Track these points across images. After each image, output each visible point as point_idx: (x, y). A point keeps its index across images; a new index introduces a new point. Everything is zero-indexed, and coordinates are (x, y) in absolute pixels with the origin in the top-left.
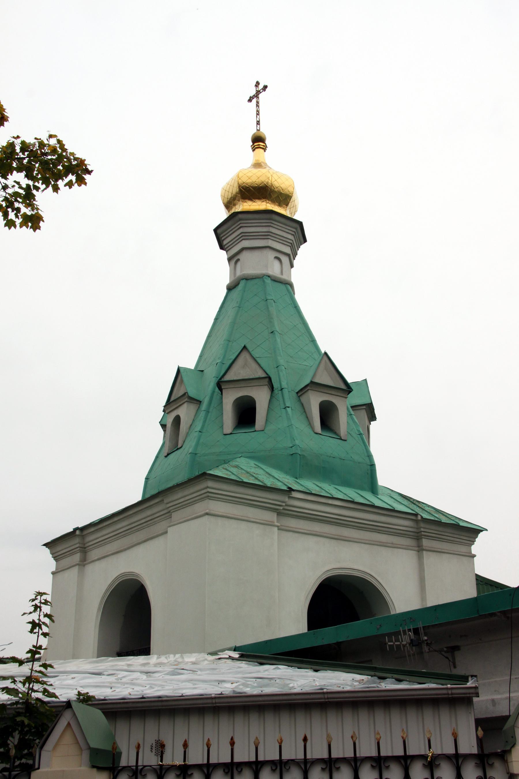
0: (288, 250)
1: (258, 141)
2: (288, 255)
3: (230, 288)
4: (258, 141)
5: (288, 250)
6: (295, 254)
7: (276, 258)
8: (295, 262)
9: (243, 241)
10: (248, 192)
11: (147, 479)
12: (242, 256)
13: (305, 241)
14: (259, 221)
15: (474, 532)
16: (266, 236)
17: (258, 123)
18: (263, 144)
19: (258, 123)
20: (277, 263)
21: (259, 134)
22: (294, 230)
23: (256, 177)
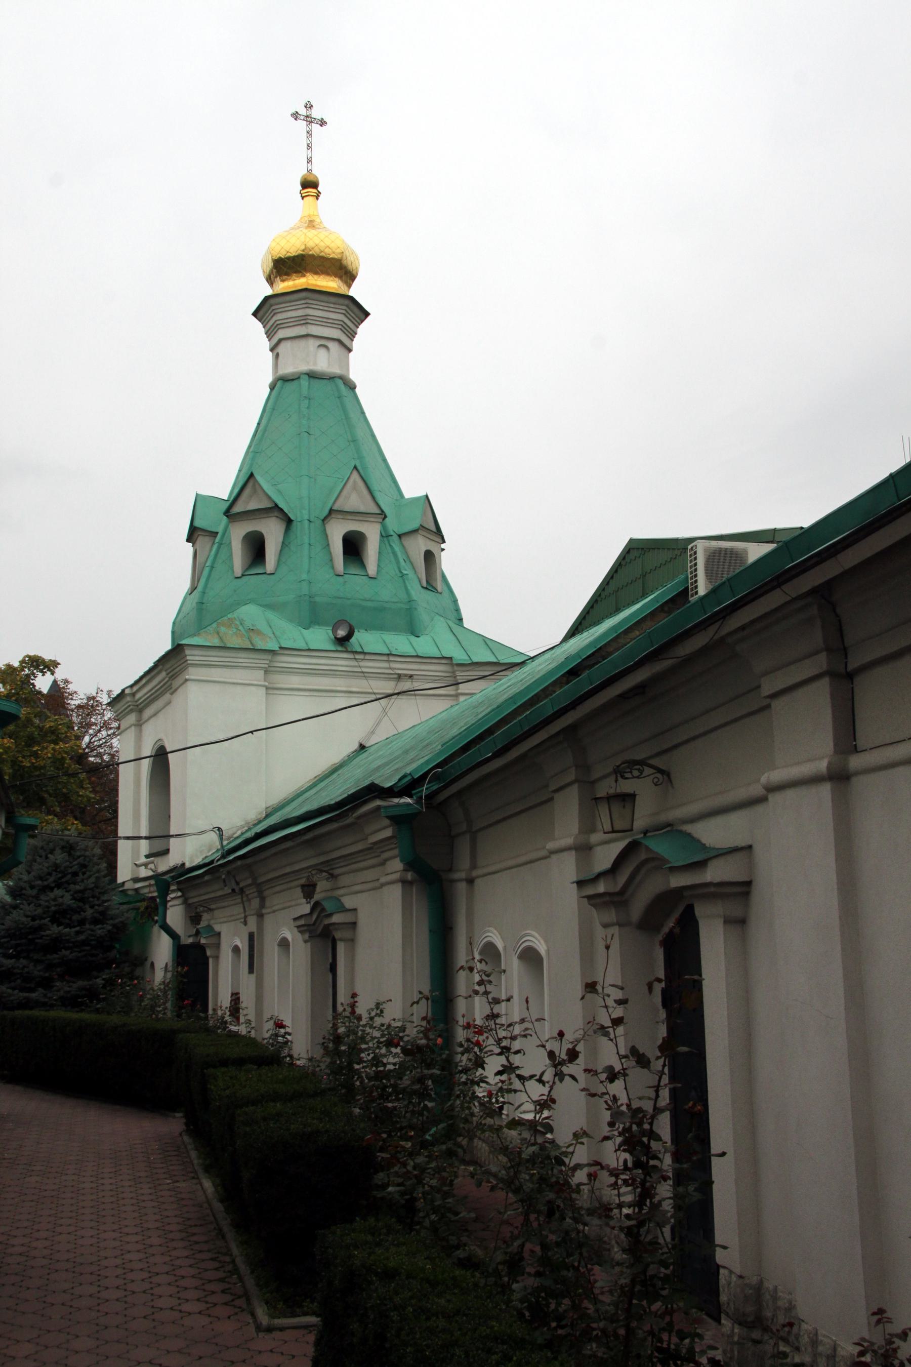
0: (336, 333)
1: (309, 184)
2: (339, 341)
3: (272, 387)
4: (309, 184)
5: (336, 333)
6: (352, 335)
7: (320, 346)
8: (357, 343)
9: (280, 331)
10: (283, 266)
11: (174, 623)
12: (280, 349)
13: (367, 314)
14: (310, 295)
15: (56, 664)
16: (304, 321)
17: (309, 161)
18: (315, 191)
19: (309, 161)
20: (323, 351)
21: (311, 178)
22: (344, 307)
23: (292, 246)
